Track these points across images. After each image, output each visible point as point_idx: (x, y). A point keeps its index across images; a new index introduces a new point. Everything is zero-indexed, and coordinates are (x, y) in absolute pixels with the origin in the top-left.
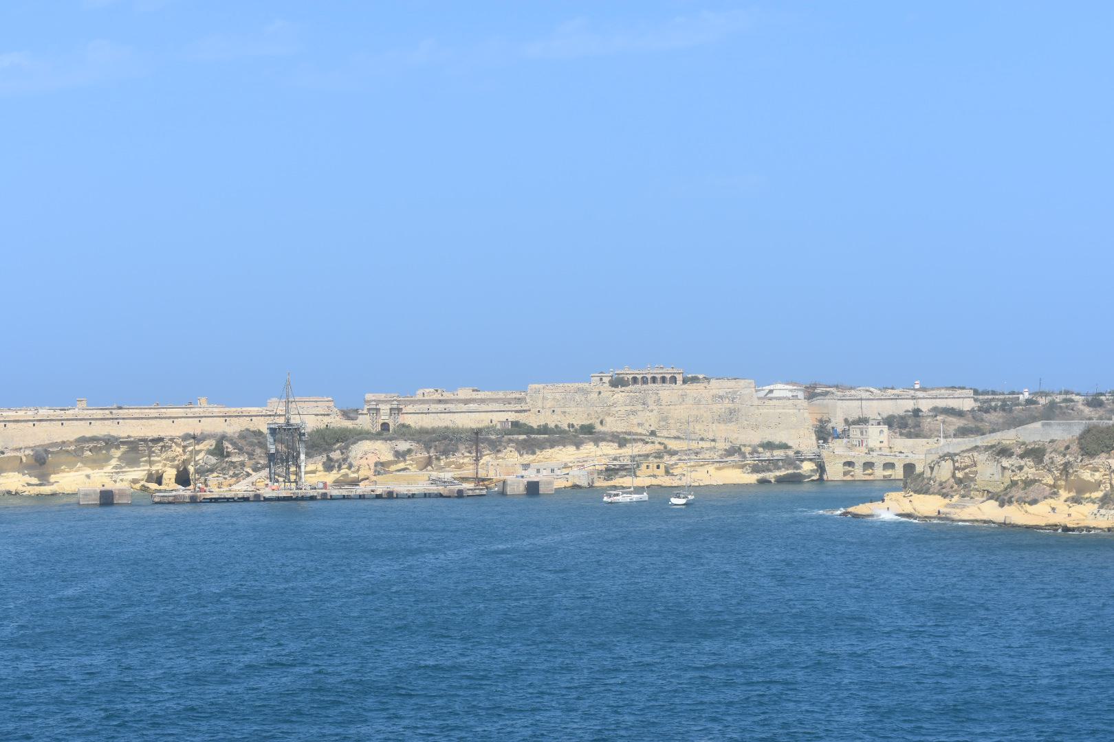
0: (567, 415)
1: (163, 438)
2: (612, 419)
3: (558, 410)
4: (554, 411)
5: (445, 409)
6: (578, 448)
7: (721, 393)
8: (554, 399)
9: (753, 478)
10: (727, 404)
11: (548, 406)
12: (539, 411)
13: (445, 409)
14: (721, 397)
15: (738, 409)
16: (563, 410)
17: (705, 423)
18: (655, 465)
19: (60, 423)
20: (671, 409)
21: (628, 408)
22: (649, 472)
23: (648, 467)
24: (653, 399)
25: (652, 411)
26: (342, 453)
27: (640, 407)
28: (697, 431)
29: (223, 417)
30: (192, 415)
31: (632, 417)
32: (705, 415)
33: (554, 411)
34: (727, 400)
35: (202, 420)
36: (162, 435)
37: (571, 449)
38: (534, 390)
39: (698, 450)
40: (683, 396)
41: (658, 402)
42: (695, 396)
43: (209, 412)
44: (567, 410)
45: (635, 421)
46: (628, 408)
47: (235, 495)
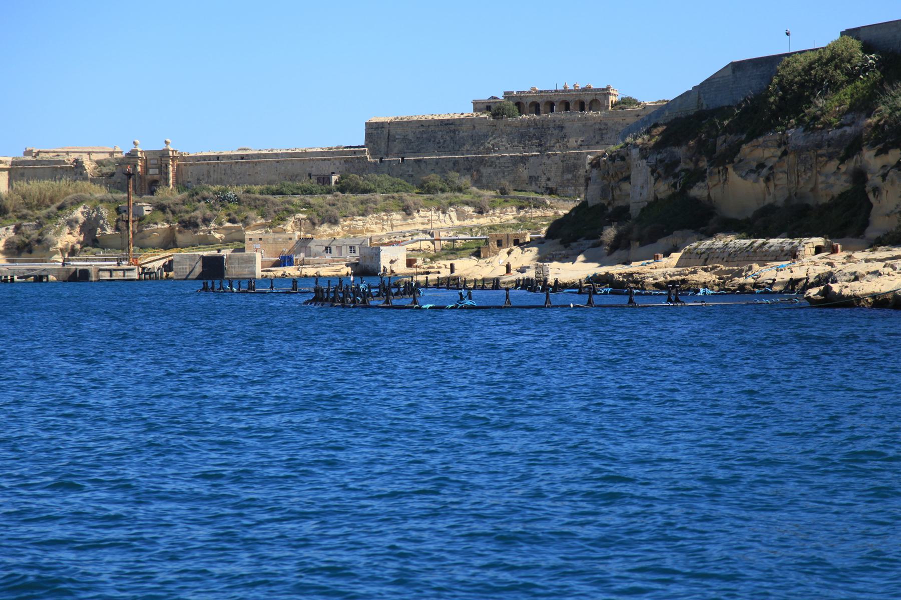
0: (423, 166)
2: (489, 170)
5: (242, 158)
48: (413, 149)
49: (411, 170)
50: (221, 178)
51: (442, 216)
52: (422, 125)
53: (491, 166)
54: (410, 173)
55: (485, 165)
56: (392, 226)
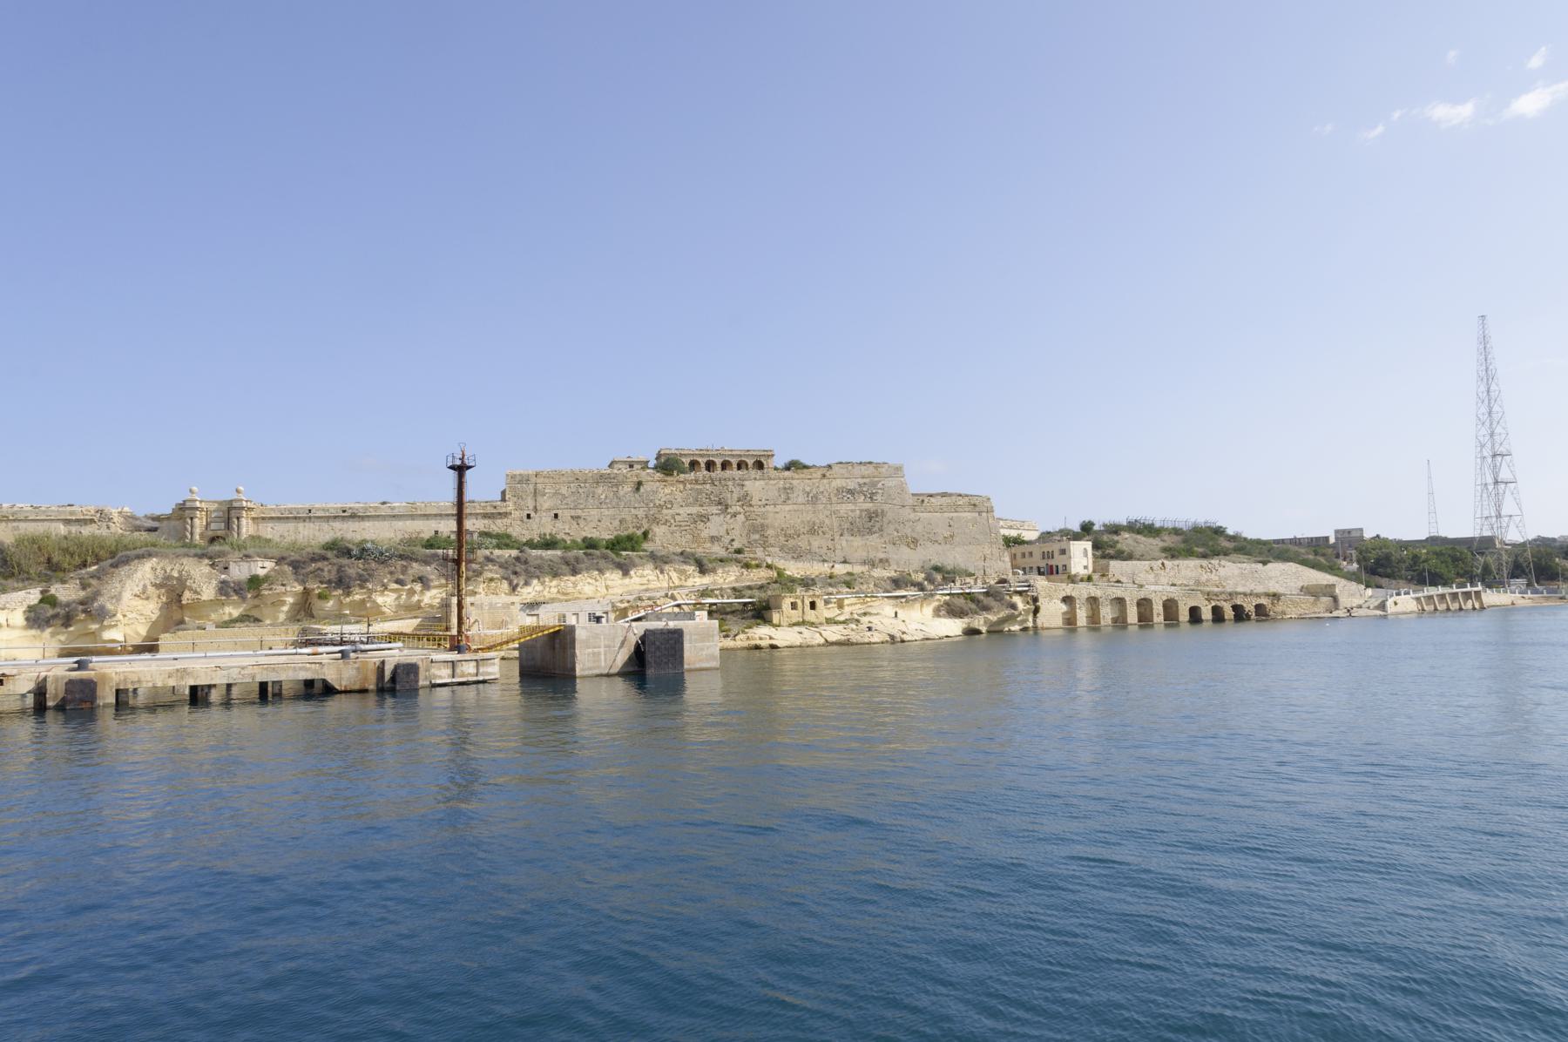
0: (582, 523)
3: (565, 514)
4: (556, 516)
5: (344, 511)
6: (626, 573)
7: (851, 485)
8: (555, 494)
9: (953, 627)
10: (863, 504)
11: (546, 506)
12: (529, 516)
13: (344, 511)
14: (851, 492)
15: (883, 511)
16: (573, 513)
18: (807, 602)
20: (767, 512)
21: (694, 510)
22: (796, 616)
23: (794, 606)
24: (735, 496)
25: (735, 515)
26: (84, 587)
27: (715, 509)
28: (814, 549)
31: (701, 525)
32: (827, 521)
33: (556, 516)
34: (863, 497)
37: (614, 577)
38: (518, 479)
39: (848, 578)
40: (788, 490)
41: (745, 499)
42: (808, 489)
44: (579, 512)
45: (705, 534)
46: (694, 510)
48: (567, 504)
49: (567, 527)
50: (314, 536)
51: (661, 576)
52: (577, 479)
54: (567, 531)
55: (658, 523)
56: (607, 587)
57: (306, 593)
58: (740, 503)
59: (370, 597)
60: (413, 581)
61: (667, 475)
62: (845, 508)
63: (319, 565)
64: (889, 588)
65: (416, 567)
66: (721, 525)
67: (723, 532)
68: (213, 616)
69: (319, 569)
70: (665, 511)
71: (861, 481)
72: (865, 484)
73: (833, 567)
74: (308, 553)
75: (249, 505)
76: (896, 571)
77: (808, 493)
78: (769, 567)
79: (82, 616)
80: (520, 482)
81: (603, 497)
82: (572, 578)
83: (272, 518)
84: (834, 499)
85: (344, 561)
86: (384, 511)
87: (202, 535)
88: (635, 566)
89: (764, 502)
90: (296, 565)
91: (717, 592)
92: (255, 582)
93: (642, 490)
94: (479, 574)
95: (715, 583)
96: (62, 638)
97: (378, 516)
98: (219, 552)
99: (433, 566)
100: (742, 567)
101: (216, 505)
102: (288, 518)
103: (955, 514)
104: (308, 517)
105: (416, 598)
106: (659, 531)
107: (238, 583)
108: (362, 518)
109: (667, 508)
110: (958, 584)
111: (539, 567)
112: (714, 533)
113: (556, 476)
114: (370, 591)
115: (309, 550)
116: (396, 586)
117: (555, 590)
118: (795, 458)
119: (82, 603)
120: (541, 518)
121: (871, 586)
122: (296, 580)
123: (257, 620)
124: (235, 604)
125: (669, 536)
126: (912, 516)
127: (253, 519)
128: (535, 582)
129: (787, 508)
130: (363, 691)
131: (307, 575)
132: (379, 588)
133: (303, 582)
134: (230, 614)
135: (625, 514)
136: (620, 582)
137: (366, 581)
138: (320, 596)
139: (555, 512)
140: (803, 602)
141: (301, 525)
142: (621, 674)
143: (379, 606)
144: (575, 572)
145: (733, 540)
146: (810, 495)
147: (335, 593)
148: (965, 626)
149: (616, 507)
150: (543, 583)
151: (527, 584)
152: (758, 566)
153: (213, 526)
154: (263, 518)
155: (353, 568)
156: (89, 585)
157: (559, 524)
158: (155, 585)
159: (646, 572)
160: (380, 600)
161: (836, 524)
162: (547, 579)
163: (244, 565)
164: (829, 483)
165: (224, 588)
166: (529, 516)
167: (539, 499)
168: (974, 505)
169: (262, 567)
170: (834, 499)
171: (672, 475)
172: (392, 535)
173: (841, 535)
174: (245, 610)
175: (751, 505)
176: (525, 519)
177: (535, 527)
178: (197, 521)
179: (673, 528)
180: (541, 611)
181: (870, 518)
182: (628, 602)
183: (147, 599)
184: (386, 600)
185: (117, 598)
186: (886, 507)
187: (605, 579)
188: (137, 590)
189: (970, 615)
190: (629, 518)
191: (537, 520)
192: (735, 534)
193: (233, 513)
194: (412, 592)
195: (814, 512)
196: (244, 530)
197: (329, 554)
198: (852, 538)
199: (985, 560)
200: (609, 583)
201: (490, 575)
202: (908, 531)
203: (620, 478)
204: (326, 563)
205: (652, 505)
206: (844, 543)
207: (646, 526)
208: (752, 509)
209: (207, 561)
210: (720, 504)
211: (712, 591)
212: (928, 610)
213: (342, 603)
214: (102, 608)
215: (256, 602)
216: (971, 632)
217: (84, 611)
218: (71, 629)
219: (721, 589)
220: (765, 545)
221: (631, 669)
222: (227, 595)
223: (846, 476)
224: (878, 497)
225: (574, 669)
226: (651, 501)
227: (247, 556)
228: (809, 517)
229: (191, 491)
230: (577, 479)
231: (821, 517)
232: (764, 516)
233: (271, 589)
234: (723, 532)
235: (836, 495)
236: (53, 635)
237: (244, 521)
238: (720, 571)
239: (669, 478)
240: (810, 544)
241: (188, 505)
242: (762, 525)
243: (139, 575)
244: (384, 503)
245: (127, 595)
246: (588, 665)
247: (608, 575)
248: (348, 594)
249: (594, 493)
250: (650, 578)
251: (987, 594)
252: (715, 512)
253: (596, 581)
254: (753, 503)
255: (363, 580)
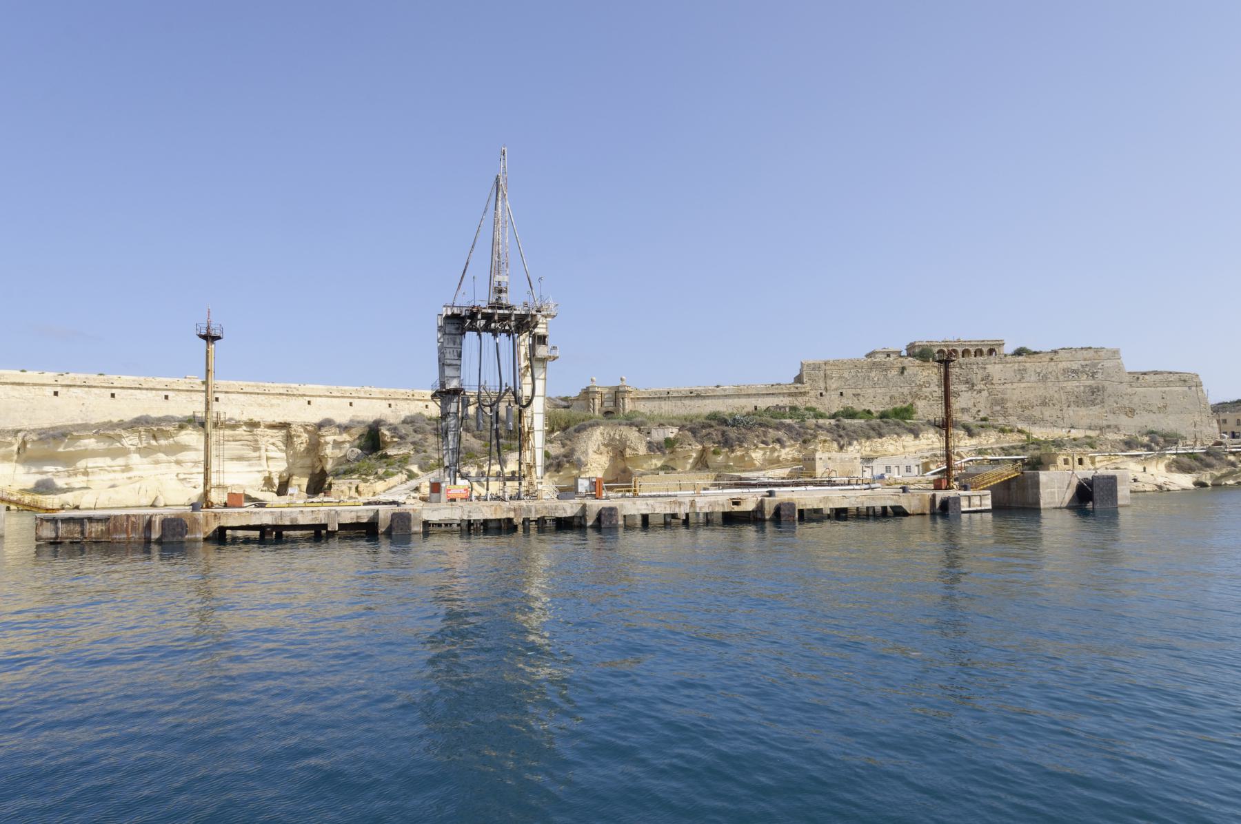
0: (861, 399)
1: (289, 424)
3: (848, 392)
4: (841, 394)
5: (691, 393)
6: (916, 436)
7: (1075, 366)
8: (840, 377)
9: (1185, 481)
11: (834, 386)
12: (821, 394)
13: (691, 393)
14: (1074, 371)
15: (1103, 387)
16: (854, 391)
17: (1057, 407)
18: (1076, 459)
19: (108, 392)
20: (1007, 388)
23: (1066, 462)
24: (979, 377)
25: (980, 391)
26: (564, 445)
29: (385, 399)
30: (339, 395)
32: (1056, 396)
33: (841, 394)
34: (1086, 376)
35: (355, 402)
36: (288, 420)
37: (908, 439)
38: (812, 366)
40: (1022, 372)
41: (987, 379)
42: (1039, 370)
43: (365, 392)
44: (859, 391)
47: (328, 514)
50: (672, 410)
53: (925, 399)
57: (704, 450)
58: (984, 382)
59: (747, 453)
60: (773, 442)
61: (924, 361)
62: (1071, 385)
63: (708, 430)
64: (1123, 448)
65: (772, 433)
66: (969, 399)
67: (970, 405)
68: (645, 466)
69: (709, 433)
70: (924, 389)
71: (1084, 363)
72: (1087, 365)
73: (1069, 431)
74: (699, 423)
75: (630, 389)
76: (1125, 435)
77: (1039, 374)
78: (1020, 431)
79: (568, 465)
80: (814, 369)
81: (876, 379)
82: (880, 440)
83: (643, 398)
84: (1061, 378)
85: (725, 428)
86: (719, 392)
87: (599, 410)
88: (922, 431)
89: (1003, 381)
90: (694, 431)
91: (989, 451)
92: (669, 443)
93: (905, 373)
94: (815, 437)
95: (980, 443)
96: (556, 479)
97: (715, 396)
98: (641, 421)
99: (783, 431)
100: (999, 432)
101: (607, 390)
102: (654, 398)
103: (1167, 389)
104: (667, 396)
105: (776, 454)
106: (920, 404)
107: (658, 443)
108: (704, 397)
109: (926, 387)
110: (1180, 446)
111: (855, 432)
112: (965, 406)
113: (837, 364)
114: (747, 450)
115: (699, 420)
116: (763, 446)
117: (868, 449)
118: (1023, 345)
119: (565, 456)
120: (830, 395)
121: (1109, 446)
122: (697, 441)
123: (673, 469)
124: (659, 458)
125: (929, 408)
126: (1129, 390)
127: (632, 398)
128: (855, 442)
129: (1023, 385)
130: (923, 514)
131: (702, 437)
132: (752, 447)
133: (701, 443)
134: (656, 465)
135: (894, 392)
136: (913, 443)
137: (742, 442)
138: (715, 453)
139: (841, 391)
140: (1073, 459)
141: (663, 403)
142: (1068, 508)
143: (753, 459)
144: (881, 436)
145: (979, 411)
146: (1041, 375)
147: (723, 450)
148: (1195, 480)
149: (887, 386)
150: (860, 444)
151: (850, 444)
152: (1011, 431)
153: (606, 404)
154: (638, 398)
155: (732, 433)
156: (566, 445)
157: (844, 400)
158: (604, 445)
159: (930, 436)
160: (753, 455)
161: (1063, 398)
162: (863, 441)
163: (661, 431)
164: (1056, 365)
165: (651, 446)
166: (821, 394)
167: (828, 381)
168: (1185, 381)
169: (672, 432)
170: (1061, 378)
171: (928, 361)
172: (725, 410)
173: (1069, 406)
174: (665, 462)
175: (992, 384)
176: (819, 397)
177: (826, 402)
178: (596, 401)
179: (931, 402)
180: (874, 464)
181: (1093, 393)
182: (927, 458)
183: (601, 454)
184: (757, 456)
185: (586, 453)
186: (1106, 384)
187: (903, 441)
188: (595, 448)
189: (1197, 471)
190: (897, 395)
191: (828, 397)
192: (981, 406)
193: (620, 395)
194: (774, 450)
195: (1045, 388)
196: (627, 407)
197: (713, 423)
198: (1078, 409)
199: (1195, 426)
200: (905, 443)
201: (823, 438)
202: (1126, 403)
203: (889, 365)
204: (712, 429)
205: (914, 385)
206: (1071, 413)
207: (910, 401)
208: (993, 387)
209: (634, 428)
210: (967, 383)
211: (986, 450)
212: (1162, 467)
213: (729, 457)
214: (579, 460)
215: (672, 456)
216: (1200, 484)
217: (568, 462)
218: (561, 473)
219: (992, 449)
220: (1005, 415)
221: (1074, 505)
222: (653, 451)
223: (1070, 359)
224: (1099, 376)
225: (1038, 503)
226: (913, 381)
227: (663, 425)
228: (1041, 392)
229: (592, 380)
230: (855, 365)
231: (1051, 392)
232: (1003, 392)
233: (682, 448)
234: (970, 405)
235: (1063, 374)
236: (550, 477)
237: (626, 401)
238: (983, 435)
239: (926, 364)
240: (1042, 414)
241: (591, 390)
242: (1002, 399)
243: (594, 438)
244: (718, 386)
245: (590, 451)
246: (1048, 501)
247: (904, 438)
248: (733, 451)
249: (869, 376)
250: (934, 440)
251: (1207, 454)
252: (963, 389)
253: (896, 442)
254: (994, 382)
255: (741, 442)
